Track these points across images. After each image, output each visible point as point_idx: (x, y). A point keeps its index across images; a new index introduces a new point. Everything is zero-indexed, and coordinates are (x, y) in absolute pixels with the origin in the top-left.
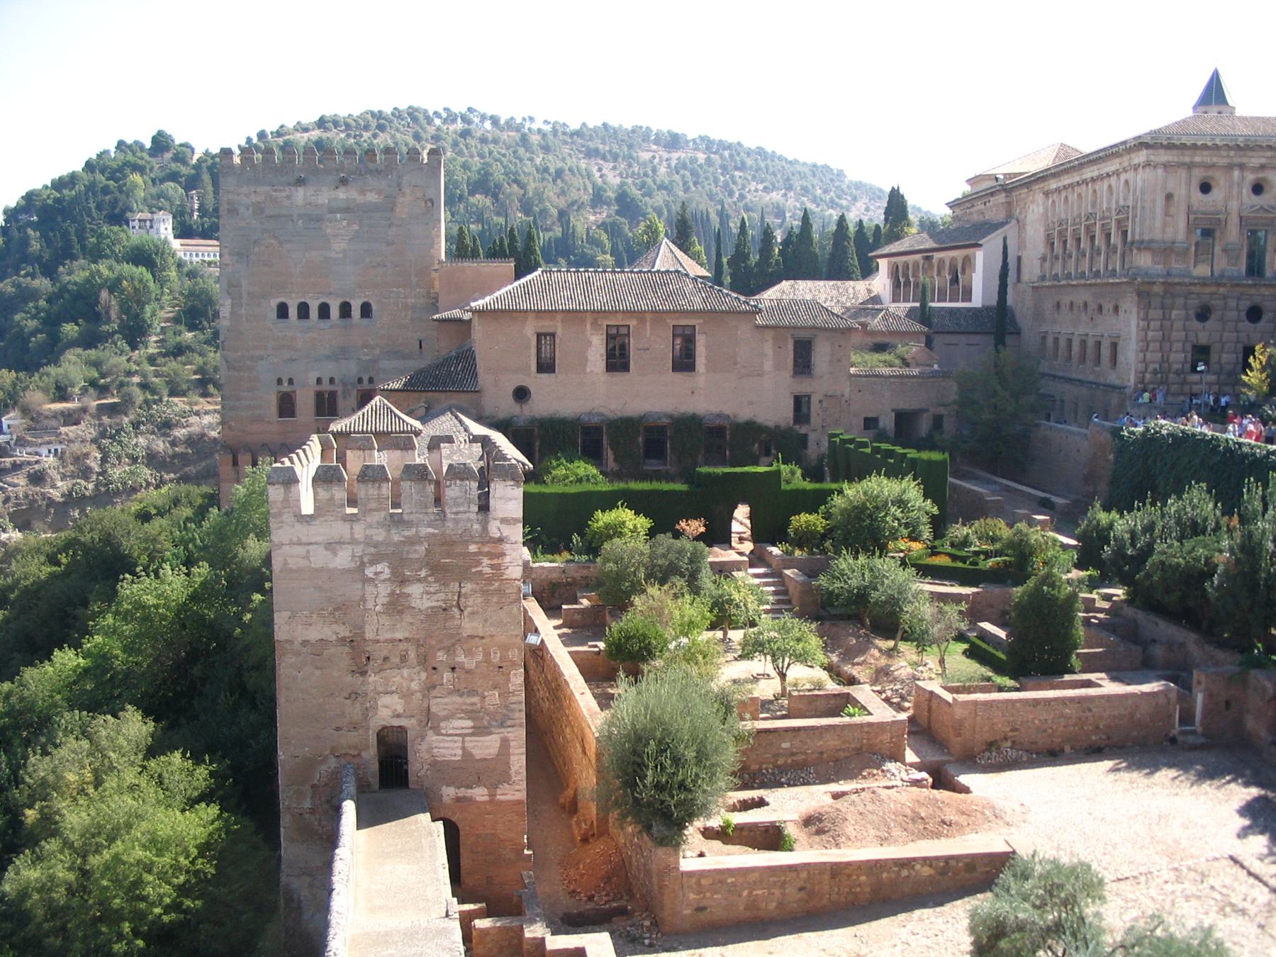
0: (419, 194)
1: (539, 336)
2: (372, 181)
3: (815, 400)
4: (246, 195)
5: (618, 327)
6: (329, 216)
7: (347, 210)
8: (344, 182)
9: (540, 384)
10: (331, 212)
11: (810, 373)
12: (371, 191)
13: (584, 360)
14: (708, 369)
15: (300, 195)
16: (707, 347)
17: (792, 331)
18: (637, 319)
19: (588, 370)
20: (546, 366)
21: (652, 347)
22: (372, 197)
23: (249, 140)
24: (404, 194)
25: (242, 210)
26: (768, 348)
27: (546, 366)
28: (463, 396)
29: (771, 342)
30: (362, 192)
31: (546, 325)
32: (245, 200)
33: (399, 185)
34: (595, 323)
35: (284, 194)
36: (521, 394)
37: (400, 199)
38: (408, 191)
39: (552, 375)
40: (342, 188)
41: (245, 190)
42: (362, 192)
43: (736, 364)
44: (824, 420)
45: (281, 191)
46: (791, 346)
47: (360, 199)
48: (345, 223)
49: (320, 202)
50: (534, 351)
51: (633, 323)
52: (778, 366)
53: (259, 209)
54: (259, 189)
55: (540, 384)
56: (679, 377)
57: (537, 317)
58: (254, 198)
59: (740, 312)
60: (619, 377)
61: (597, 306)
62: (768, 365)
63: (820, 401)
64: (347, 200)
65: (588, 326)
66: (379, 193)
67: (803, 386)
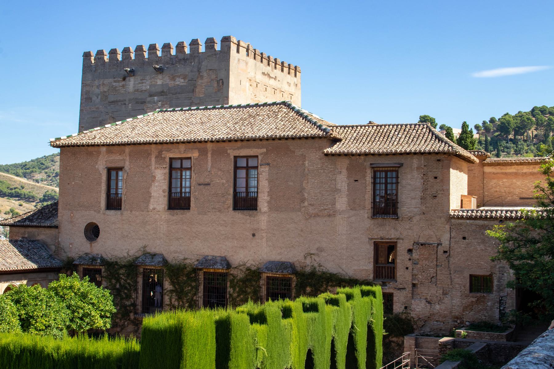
0: (213, 77)
1: (109, 170)
2: (181, 69)
3: (402, 248)
4: (98, 87)
5: (181, 159)
6: (149, 99)
7: (162, 93)
8: (160, 71)
9: (108, 220)
10: (151, 95)
11: (395, 213)
12: (179, 77)
13: (147, 196)
14: (274, 207)
15: (132, 83)
16: (270, 181)
17: (371, 160)
18: (199, 150)
19: (151, 207)
20: (114, 203)
21: (212, 181)
22: (180, 82)
23: (484, 123)
24: (202, 77)
25: (94, 98)
26: (342, 181)
27: (114, 203)
28: (48, 231)
29: (344, 172)
30: (173, 78)
31: (116, 159)
32: (97, 91)
33: (199, 71)
34: (159, 157)
35: (121, 84)
36: (93, 232)
37: (200, 82)
38: (205, 74)
39: (119, 212)
40: (160, 76)
41: (96, 83)
42: (173, 78)
43: (303, 200)
44: (414, 276)
45: (118, 81)
46: (369, 179)
47: (171, 83)
48: (160, 104)
49: (144, 88)
50: (104, 187)
51: (195, 155)
52: (353, 205)
53: (104, 96)
54: (106, 81)
55: (108, 220)
56: (239, 216)
57: (108, 152)
58: (102, 89)
59: (307, 138)
60: (179, 215)
61: (163, 138)
62: (342, 203)
63: (410, 251)
64: (162, 85)
65: (153, 159)
66: (184, 78)
67: (388, 230)
